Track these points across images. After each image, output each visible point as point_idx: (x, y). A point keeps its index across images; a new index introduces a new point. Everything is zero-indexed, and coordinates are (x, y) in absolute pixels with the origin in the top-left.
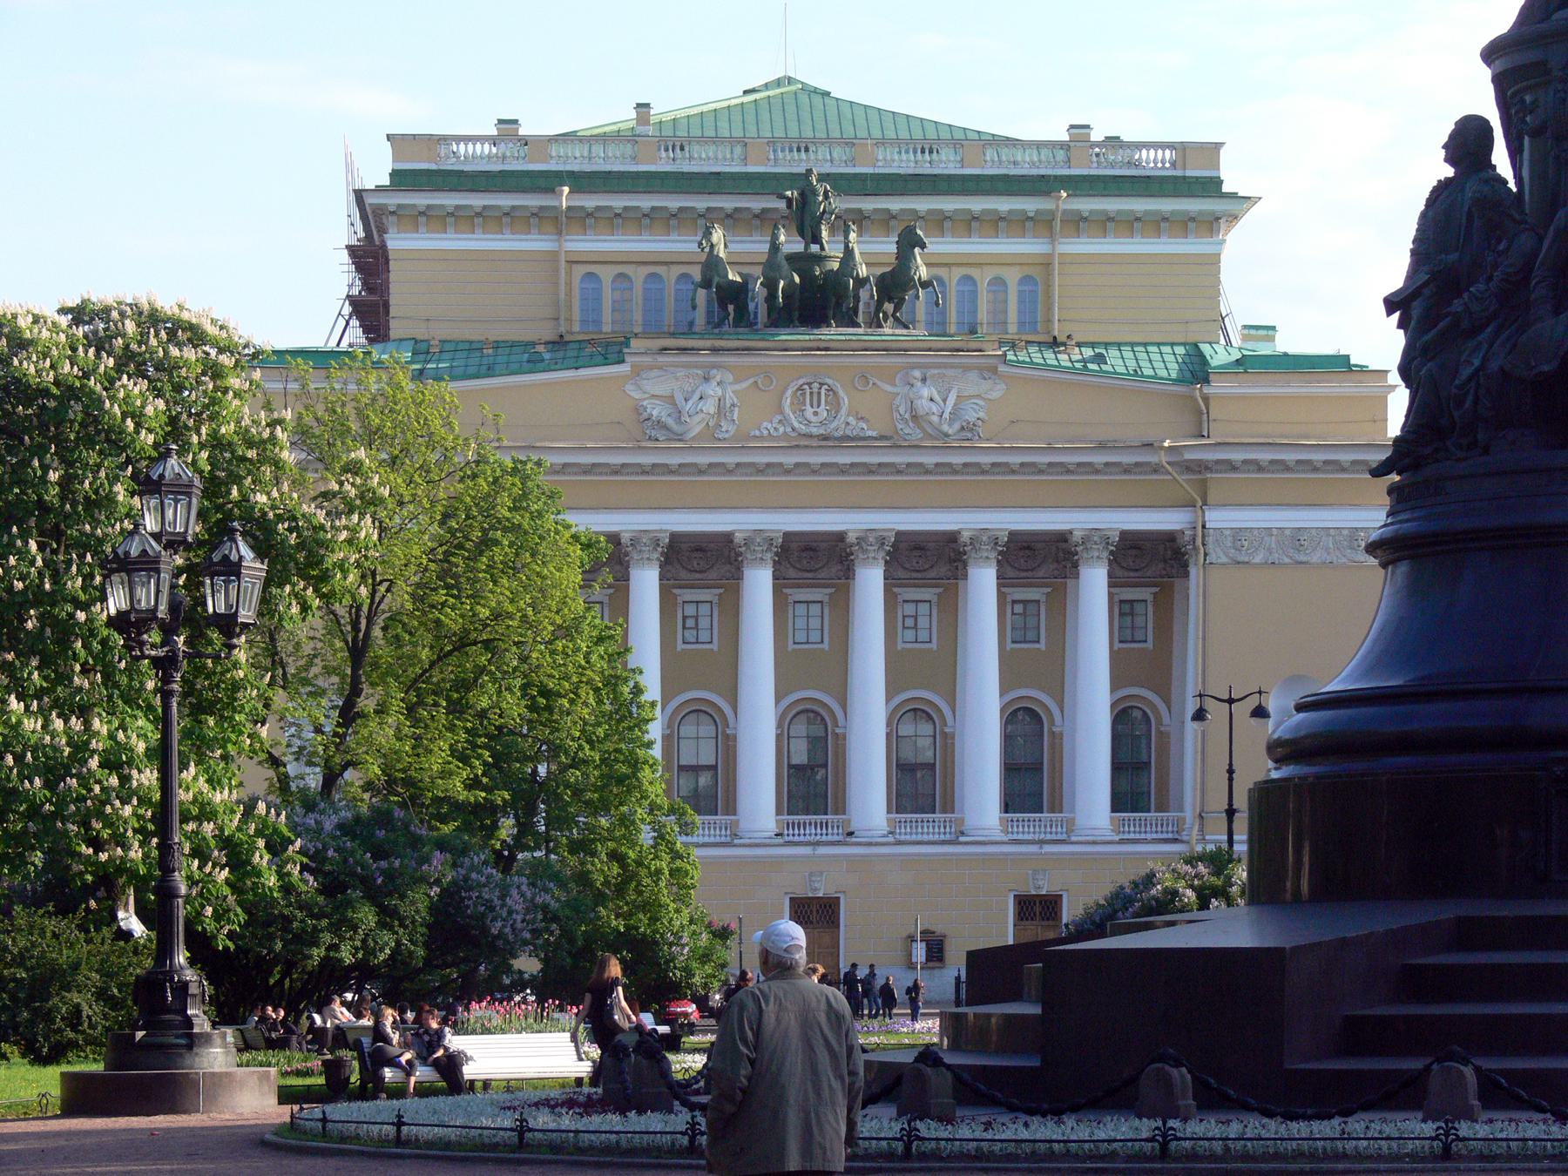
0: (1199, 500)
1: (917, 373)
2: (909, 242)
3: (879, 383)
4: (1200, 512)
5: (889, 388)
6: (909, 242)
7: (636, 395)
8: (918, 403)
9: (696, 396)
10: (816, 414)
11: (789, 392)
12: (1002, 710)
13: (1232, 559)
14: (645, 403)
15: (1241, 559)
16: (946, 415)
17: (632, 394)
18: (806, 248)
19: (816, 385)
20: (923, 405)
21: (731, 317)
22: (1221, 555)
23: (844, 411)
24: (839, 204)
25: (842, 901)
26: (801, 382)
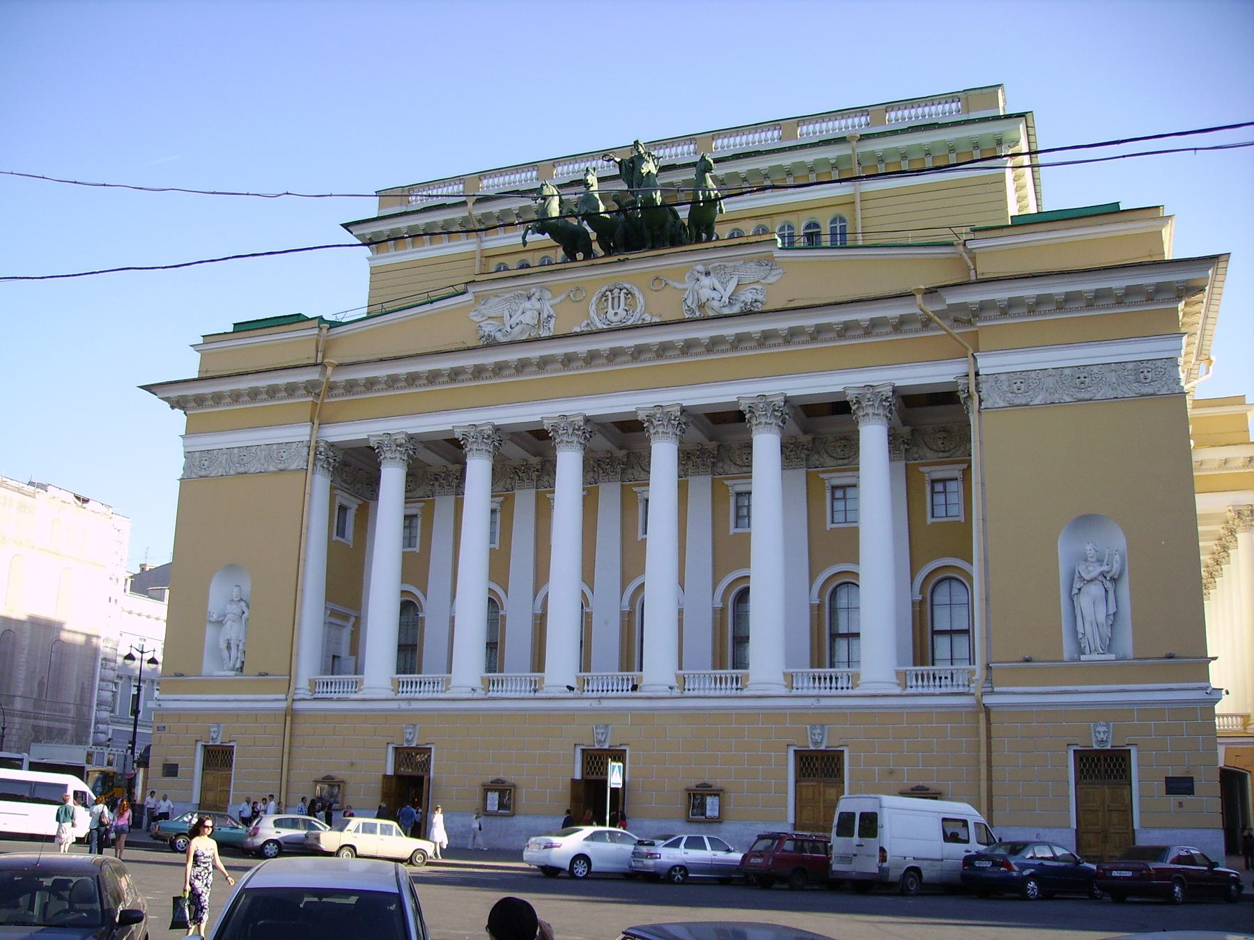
0: (969, 349)
5: (678, 286)
7: (476, 319)
9: (521, 311)
10: (616, 314)
11: (594, 299)
14: (481, 324)
15: (1017, 402)
19: (617, 291)
20: (706, 293)
22: (998, 400)
26: (604, 289)
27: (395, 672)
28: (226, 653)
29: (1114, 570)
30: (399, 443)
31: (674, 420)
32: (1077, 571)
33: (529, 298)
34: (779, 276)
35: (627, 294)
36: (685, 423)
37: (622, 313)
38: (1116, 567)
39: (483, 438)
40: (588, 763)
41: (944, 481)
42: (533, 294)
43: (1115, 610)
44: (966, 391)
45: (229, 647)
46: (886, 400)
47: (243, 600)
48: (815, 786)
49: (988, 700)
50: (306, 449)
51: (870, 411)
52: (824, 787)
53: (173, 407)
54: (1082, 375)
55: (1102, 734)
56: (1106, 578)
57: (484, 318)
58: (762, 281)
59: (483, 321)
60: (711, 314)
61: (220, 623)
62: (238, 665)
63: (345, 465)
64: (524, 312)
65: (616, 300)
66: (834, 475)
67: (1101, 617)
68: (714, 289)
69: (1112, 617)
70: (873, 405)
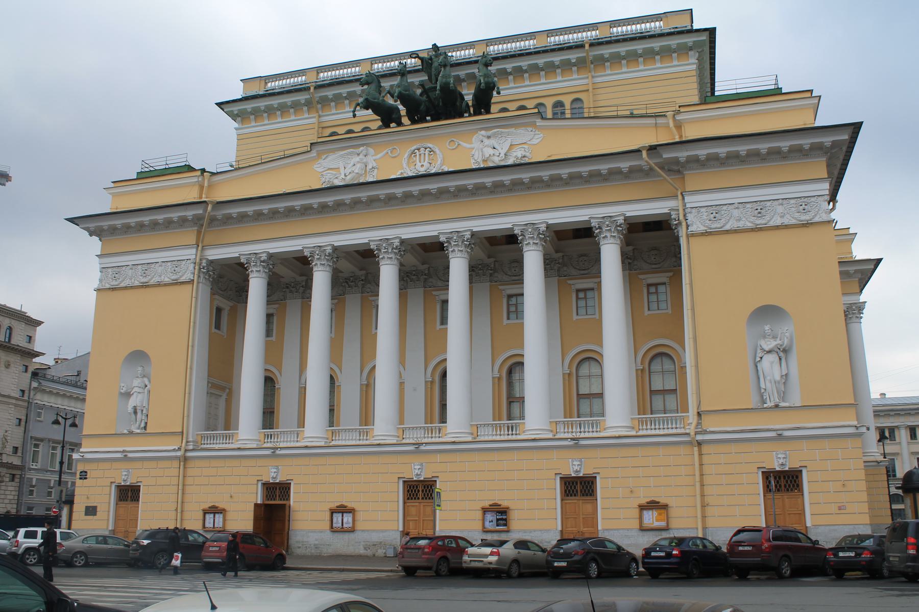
1: (483, 132)
3: (460, 142)
4: (680, 197)
7: (320, 170)
8: (485, 150)
9: (352, 164)
10: (422, 166)
13: (707, 227)
19: (422, 149)
22: (700, 225)
26: (413, 148)
27: (261, 427)
28: (133, 416)
29: (785, 343)
30: (262, 260)
31: (467, 241)
32: (759, 345)
33: (358, 155)
34: (540, 140)
35: (430, 152)
36: (473, 244)
37: (426, 164)
38: (786, 342)
39: (326, 255)
40: (408, 491)
41: (656, 285)
42: (362, 152)
43: (786, 372)
44: (677, 219)
45: (135, 412)
46: (620, 226)
47: (146, 377)
48: (575, 503)
49: (699, 437)
50: (192, 265)
51: (608, 234)
52: (582, 503)
53: (91, 235)
54: (760, 207)
55: (782, 459)
56: (779, 349)
57: (325, 169)
58: (528, 142)
59: (323, 172)
60: (491, 165)
61: (128, 395)
62: (143, 425)
63: (221, 278)
64: (355, 165)
65: (422, 155)
67: (778, 378)
68: (494, 148)
69: (784, 377)
70: (610, 229)
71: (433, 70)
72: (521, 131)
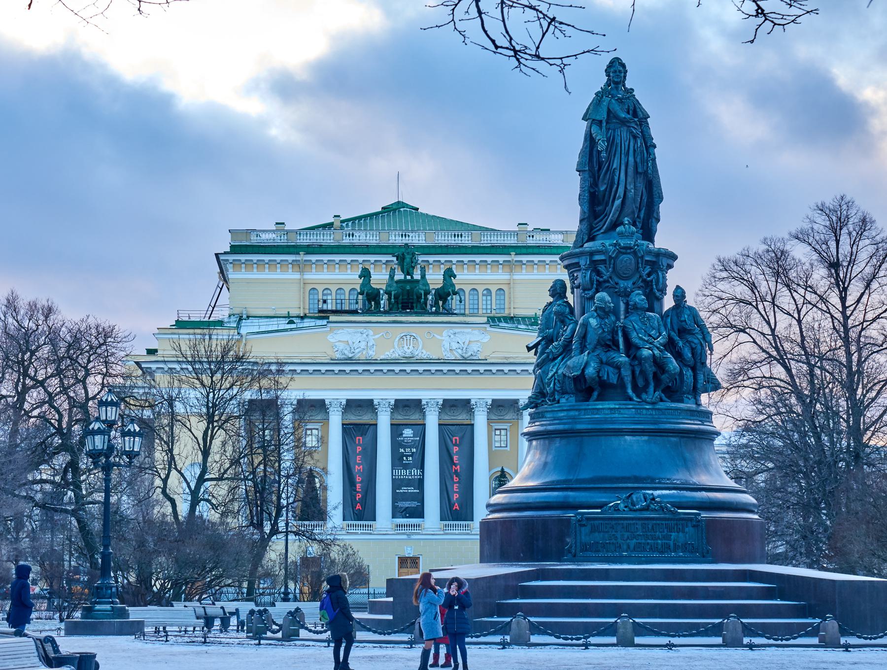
1: (451, 331)
2: (449, 274)
6: (449, 274)
7: (332, 340)
11: (397, 339)
12: (490, 478)
16: (464, 349)
17: (330, 340)
18: (405, 277)
19: (408, 337)
21: (373, 307)
23: (420, 347)
24: (421, 258)
25: (421, 558)
26: (402, 335)
37: (411, 347)
65: (408, 341)
66: (496, 424)
71: (405, 264)
72: (476, 332)
